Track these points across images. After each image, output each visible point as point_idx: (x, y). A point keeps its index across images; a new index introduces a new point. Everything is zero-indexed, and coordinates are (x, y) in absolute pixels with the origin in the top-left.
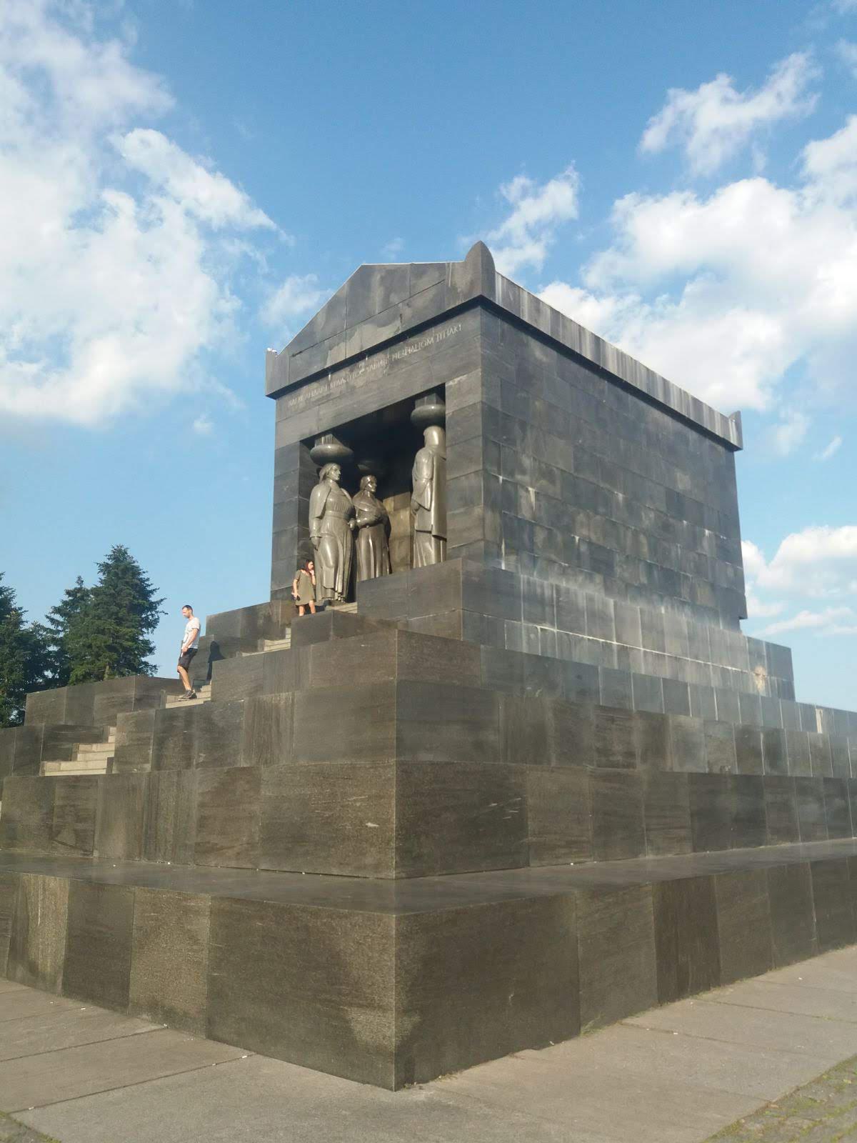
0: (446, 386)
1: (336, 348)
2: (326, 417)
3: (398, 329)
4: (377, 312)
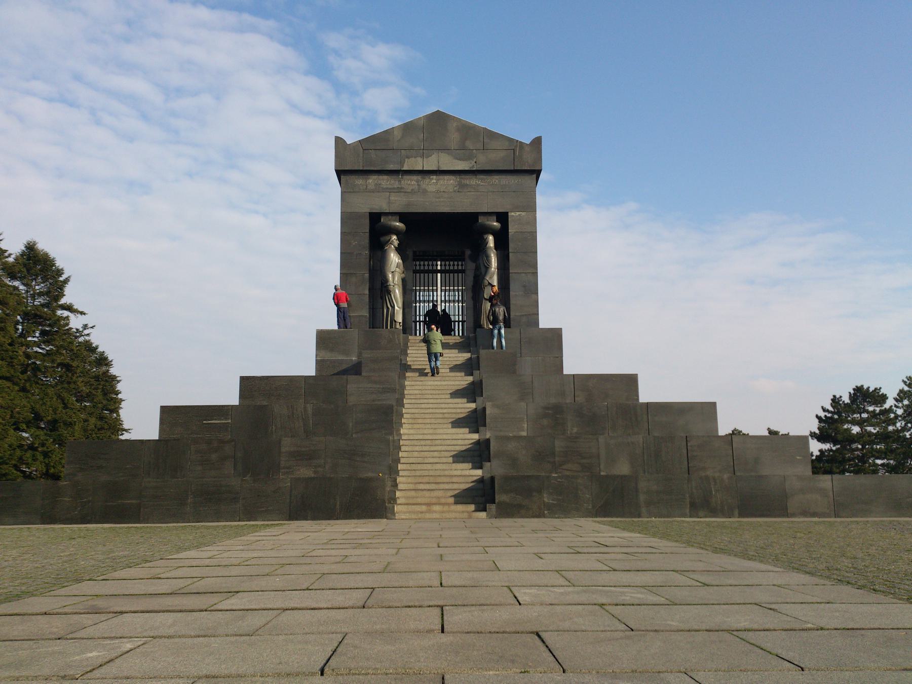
1: (413, 159)
2: (398, 203)
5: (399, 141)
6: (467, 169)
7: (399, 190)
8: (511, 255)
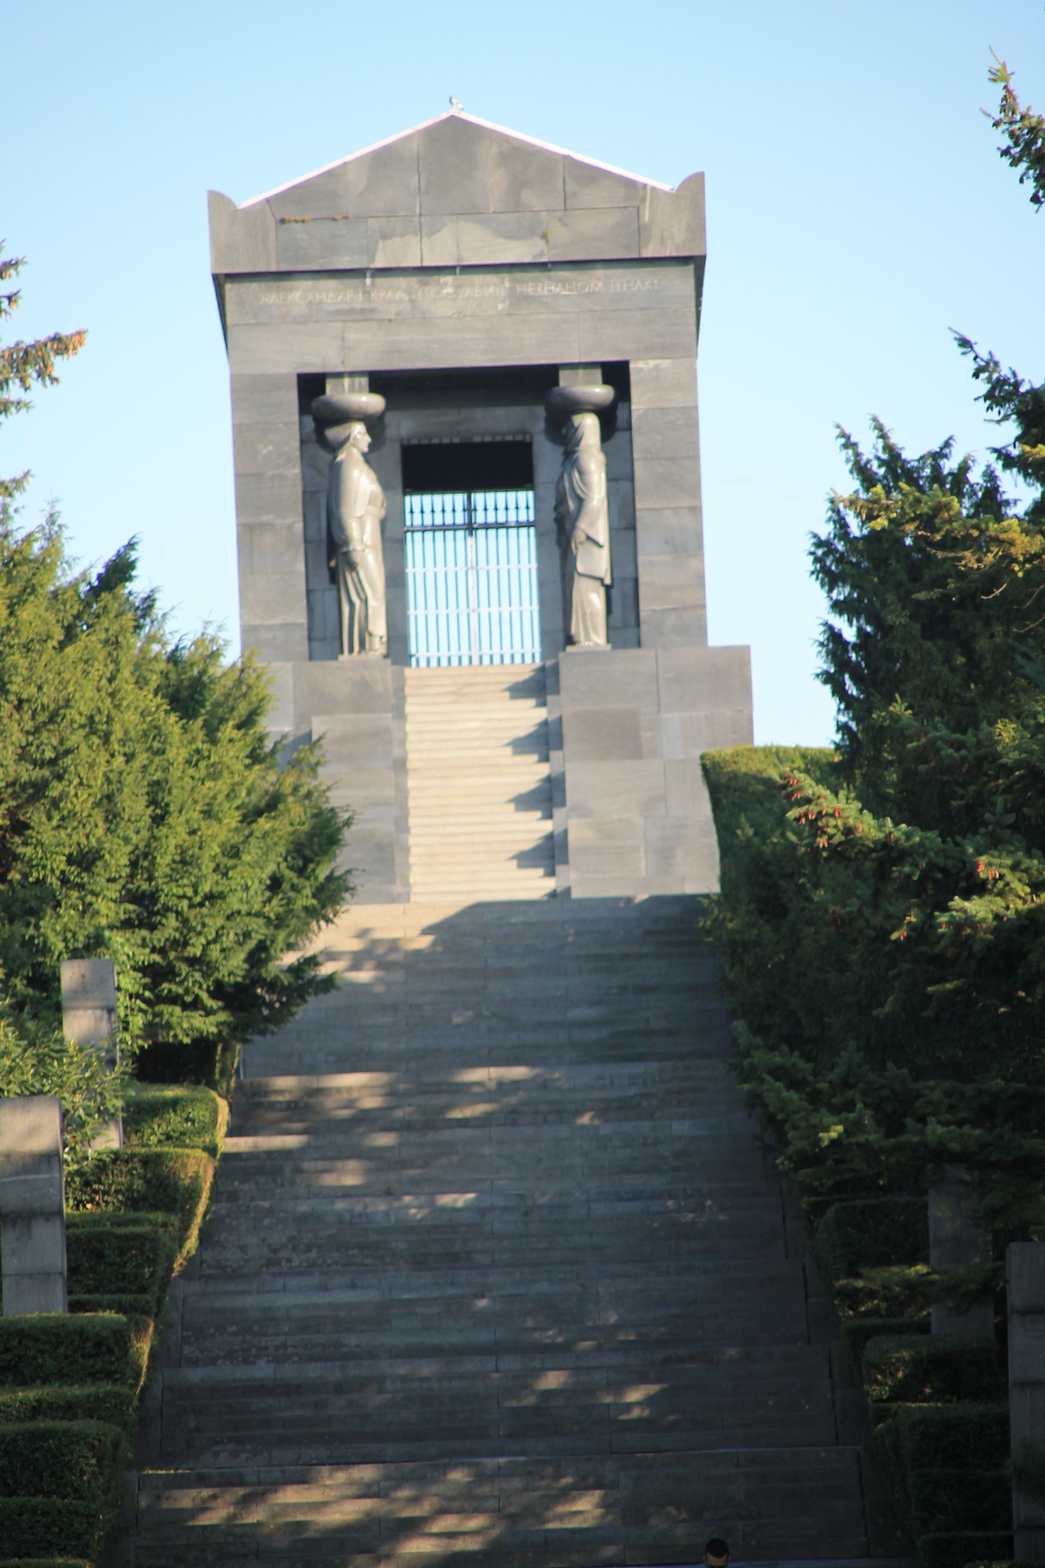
0: (632, 366)
1: (397, 240)
3: (541, 254)
4: (492, 209)
5: (361, 194)
6: (526, 259)
7: (364, 315)
8: (638, 466)
